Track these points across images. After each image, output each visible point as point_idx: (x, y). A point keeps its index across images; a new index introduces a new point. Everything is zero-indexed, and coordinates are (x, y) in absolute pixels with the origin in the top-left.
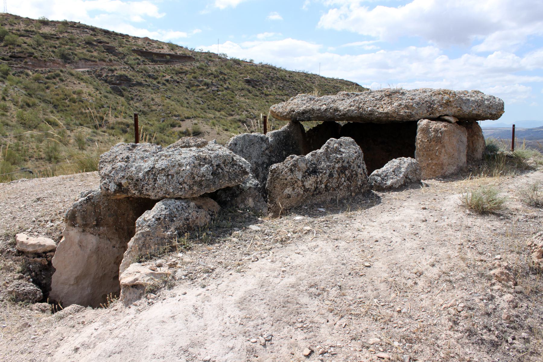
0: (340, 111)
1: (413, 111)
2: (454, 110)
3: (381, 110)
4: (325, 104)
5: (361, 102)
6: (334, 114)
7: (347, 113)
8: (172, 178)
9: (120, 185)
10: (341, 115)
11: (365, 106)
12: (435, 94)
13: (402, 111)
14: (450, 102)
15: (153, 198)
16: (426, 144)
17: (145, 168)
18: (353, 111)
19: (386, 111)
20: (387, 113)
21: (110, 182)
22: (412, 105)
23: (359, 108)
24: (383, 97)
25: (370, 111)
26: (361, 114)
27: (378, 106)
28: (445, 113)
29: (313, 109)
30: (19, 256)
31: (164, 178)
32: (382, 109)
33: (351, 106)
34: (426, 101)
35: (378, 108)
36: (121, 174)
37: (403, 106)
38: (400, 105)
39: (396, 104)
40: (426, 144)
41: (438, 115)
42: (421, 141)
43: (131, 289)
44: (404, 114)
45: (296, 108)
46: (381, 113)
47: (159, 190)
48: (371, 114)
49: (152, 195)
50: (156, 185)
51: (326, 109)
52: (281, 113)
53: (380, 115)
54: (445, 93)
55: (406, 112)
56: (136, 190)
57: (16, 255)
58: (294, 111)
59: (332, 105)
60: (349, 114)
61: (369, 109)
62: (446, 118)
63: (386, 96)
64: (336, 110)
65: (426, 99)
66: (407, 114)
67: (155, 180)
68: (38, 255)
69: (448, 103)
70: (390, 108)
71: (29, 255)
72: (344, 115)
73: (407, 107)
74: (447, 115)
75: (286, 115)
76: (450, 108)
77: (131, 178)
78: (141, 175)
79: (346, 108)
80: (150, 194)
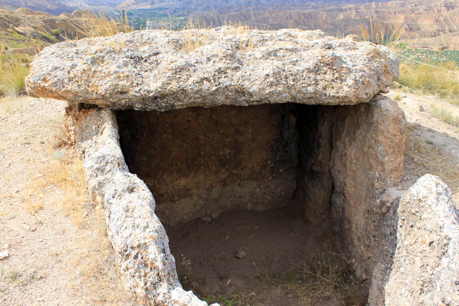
0: (251, 95)
7: (266, 98)
18: (280, 93)
29: (184, 91)
32: (334, 91)
35: (325, 89)
45: (132, 85)
46: (334, 97)
61: (311, 89)
64: (241, 91)
70: (346, 89)
75: (96, 99)
79: (264, 89)
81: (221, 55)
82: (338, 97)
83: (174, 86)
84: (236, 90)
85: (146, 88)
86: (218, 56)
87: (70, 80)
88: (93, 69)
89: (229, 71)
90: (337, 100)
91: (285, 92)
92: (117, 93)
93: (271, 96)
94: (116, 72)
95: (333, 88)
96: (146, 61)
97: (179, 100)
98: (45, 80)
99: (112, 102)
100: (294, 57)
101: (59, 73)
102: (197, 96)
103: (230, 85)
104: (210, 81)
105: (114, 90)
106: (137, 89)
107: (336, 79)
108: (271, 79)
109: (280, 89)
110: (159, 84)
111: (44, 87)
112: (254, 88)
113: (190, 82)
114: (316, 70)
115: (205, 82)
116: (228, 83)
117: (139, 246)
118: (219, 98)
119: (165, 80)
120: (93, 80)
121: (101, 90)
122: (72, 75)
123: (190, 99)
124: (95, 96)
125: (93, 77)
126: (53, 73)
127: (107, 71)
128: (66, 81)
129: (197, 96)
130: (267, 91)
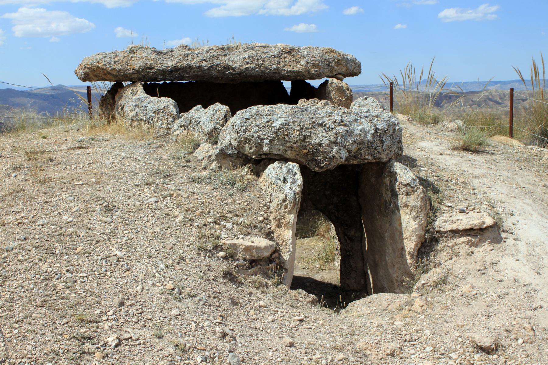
0: (234, 69)
1: (320, 69)
2: (345, 68)
3: (290, 69)
4: (205, 60)
5: (258, 60)
6: (224, 73)
7: (244, 72)
8: (393, 137)
9: (349, 151)
10: (235, 74)
11: (266, 64)
12: (326, 53)
13: (313, 70)
14: (339, 60)
15: (385, 160)
16: (344, 102)
17: (369, 130)
18: (253, 69)
19: (295, 69)
20: (298, 72)
21: (340, 150)
22: (318, 64)
23: (259, 65)
24: (282, 54)
25: (275, 69)
26: (263, 72)
27: (283, 64)
28: (339, 71)
29: (190, 67)
30: (253, 267)
31: (389, 138)
32: (291, 68)
33: (247, 63)
34: (325, 60)
35: (284, 66)
36: (350, 140)
37: (311, 65)
38: (307, 63)
39: (303, 62)
40: (344, 102)
41: (334, 74)
42: (339, 100)
43: (490, 229)
44: (316, 73)
46: (291, 71)
47: (388, 152)
48: (276, 73)
49: (384, 158)
50: (384, 147)
51: (211, 66)
52: (119, 71)
53: (289, 74)
54: (331, 51)
55: (316, 71)
56: (369, 154)
57: (250, 268)
58: (151, 68)
59: (217, 62)
60: (248, 73)
61: (274, 66)
62: (340, 76)
63: (286, 53)
64: (227, 67)
65: (324, 57)
66: (318, 72)
67: (382, 142)
68: (270, 260)
69: (338, 62)
70: (299, 66)
71: (262, 263)
72: (240, 74)
73: (313, 65)
74: (339, 74)
75: (133, 73)
76: (341, 67)
77: (362, 143)
78: (369, 137)
79: (241, 66)
80: (382, 156)
81: (215, 48)
82: (294, 72)
83: (183, 63)
84: (224, 67)
85: (166, 65)
86: (213, 49)
87: (115, 62)
88: (131, 56)
89: (220, 57)
90: (294, 74)
91: (256, 68)
92: (147, 68)
93: (247, 70)
94: (146, 56)
95: (290, 66)
96: (165, 54)
97: (187, 73)
98: (98, 62)
99: (142, 75)
100: (265, 50)
101: (108, 60)
102: (198, 70)
103: (220, 64)
104: (207, 62)
105: (145, 66)
106: (160, 66)
107: (293, 61)
108: (248, 60)
109: (253, 66)
110: (174, 63)
111: (98, 67)
112: (236, 66)
113: (194, 62)
114: (279, 56)
115: (204, 62)
116: (218, 63)
117: (164, 107)
118: (213, 72)
119: (178, 61)
120: (131, 62)
121: (137, 67)
122: (116, 59)
123: (194, 72)
124: (131, 71)
125: (131, 60)
126: (104, 59)
127: (140, 57)
128: (113, 63)
129: (198, 70)
130: (245, 66)
